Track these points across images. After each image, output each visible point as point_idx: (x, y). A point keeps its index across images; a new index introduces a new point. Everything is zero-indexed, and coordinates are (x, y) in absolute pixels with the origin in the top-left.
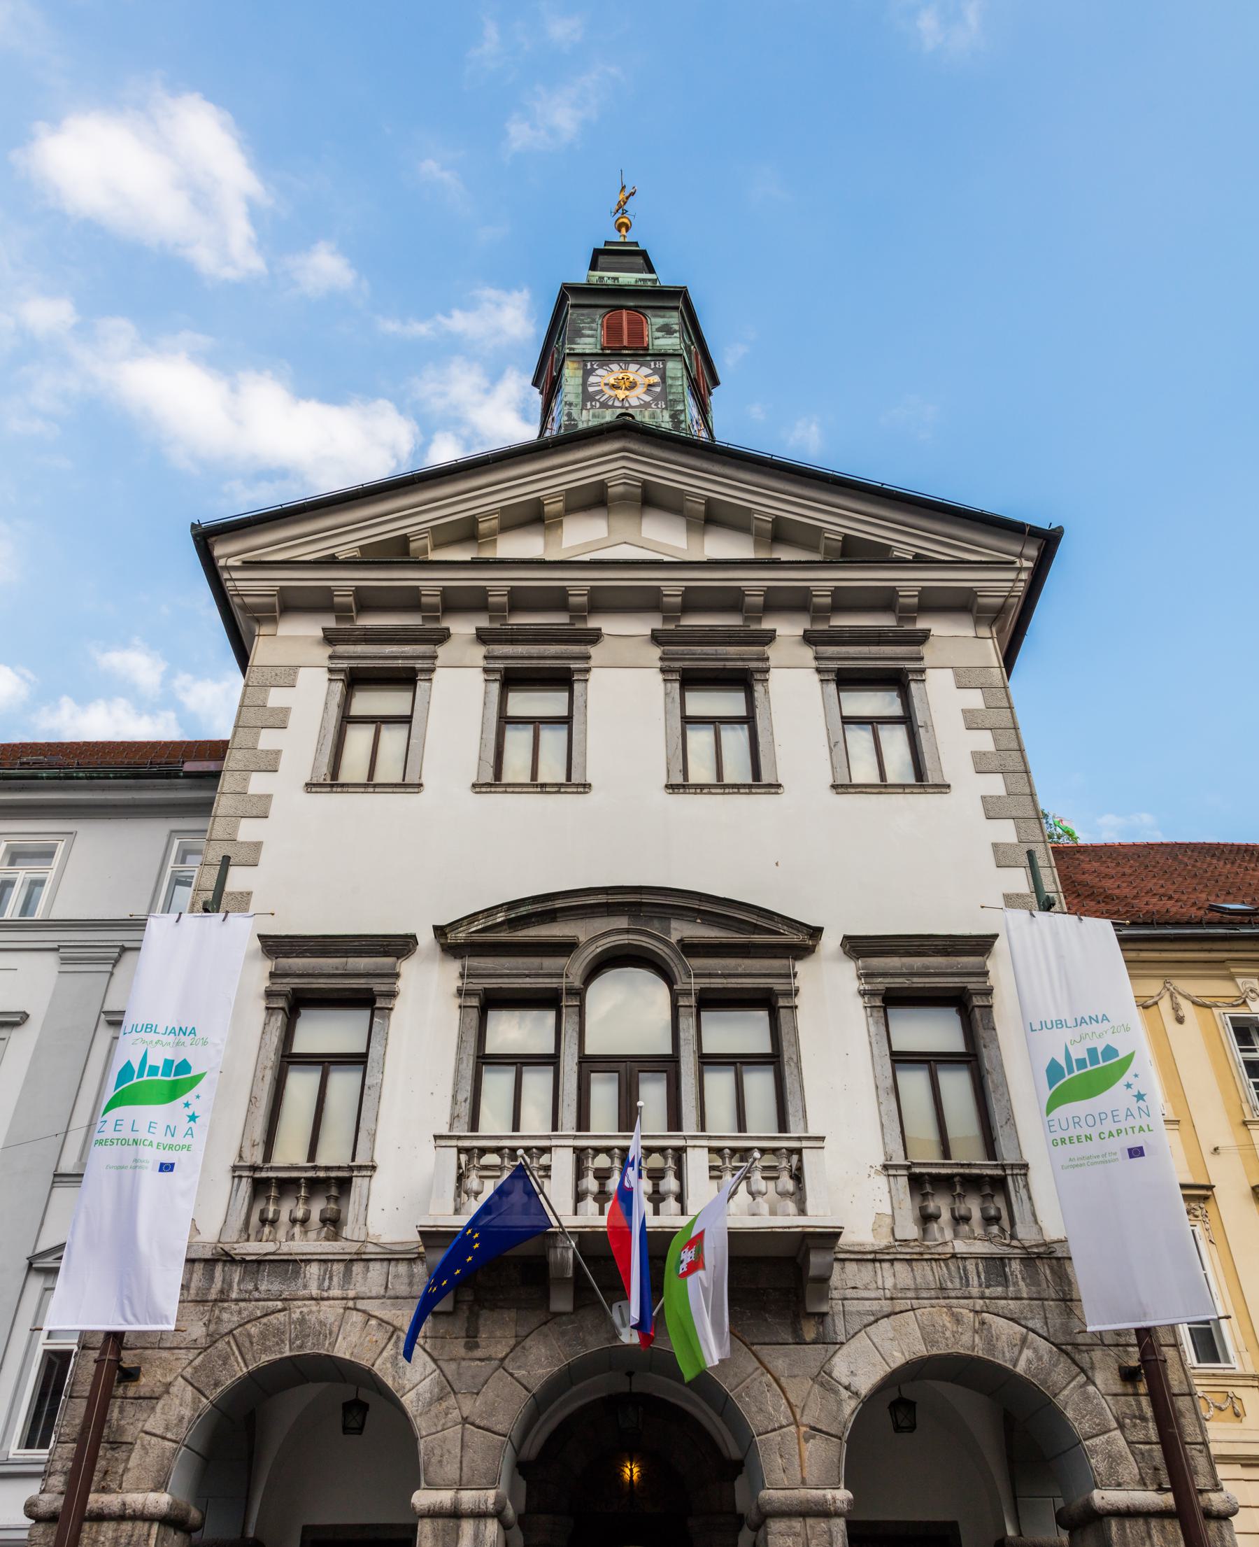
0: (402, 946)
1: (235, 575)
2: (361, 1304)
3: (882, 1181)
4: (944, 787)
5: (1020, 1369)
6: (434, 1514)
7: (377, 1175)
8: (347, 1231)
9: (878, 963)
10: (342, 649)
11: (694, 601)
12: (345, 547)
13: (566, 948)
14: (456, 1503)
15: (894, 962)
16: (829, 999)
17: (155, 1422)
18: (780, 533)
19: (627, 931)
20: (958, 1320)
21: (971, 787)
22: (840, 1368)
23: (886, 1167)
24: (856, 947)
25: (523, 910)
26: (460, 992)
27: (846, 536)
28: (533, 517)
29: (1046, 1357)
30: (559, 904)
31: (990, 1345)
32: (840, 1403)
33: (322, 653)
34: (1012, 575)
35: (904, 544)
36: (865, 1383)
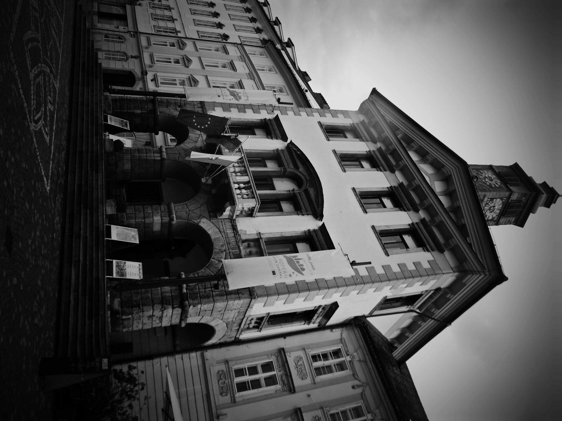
3: (255, 232)
5: (212, 259)
11: (418, 190)
13: (296, 167)
14: (163, 152)
15: (321, 237)
17: (172, 110)
18: (456, 210)
19: (306, 179)
20: (222, 246)
22: (204, 220)
23: (260, 233)
24: (323, 228)
25: (303, 157)
27: (465, 224)
28: (423, 155)
29: (217, 266)
30: (307, 164)
31: (216, 253)
32: (195, 219)
34: (479, 269)
35: (472, 238)
36: (201, 225)
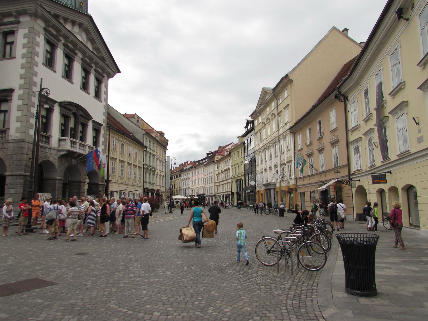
0: (55, 102)
1: (38, 6)
2: (53, 155)
4: (101, 102)
6: (59, 180)
7: (53, 137)
8: (50, 144)
9: (95, 125)
10: (47, 34)
12: (53, 11)
13: (70, 110)
16: (90, 126)
18: (97, 49)
21: (104, 103)
26: (60, 113)
33: (43, 32)
